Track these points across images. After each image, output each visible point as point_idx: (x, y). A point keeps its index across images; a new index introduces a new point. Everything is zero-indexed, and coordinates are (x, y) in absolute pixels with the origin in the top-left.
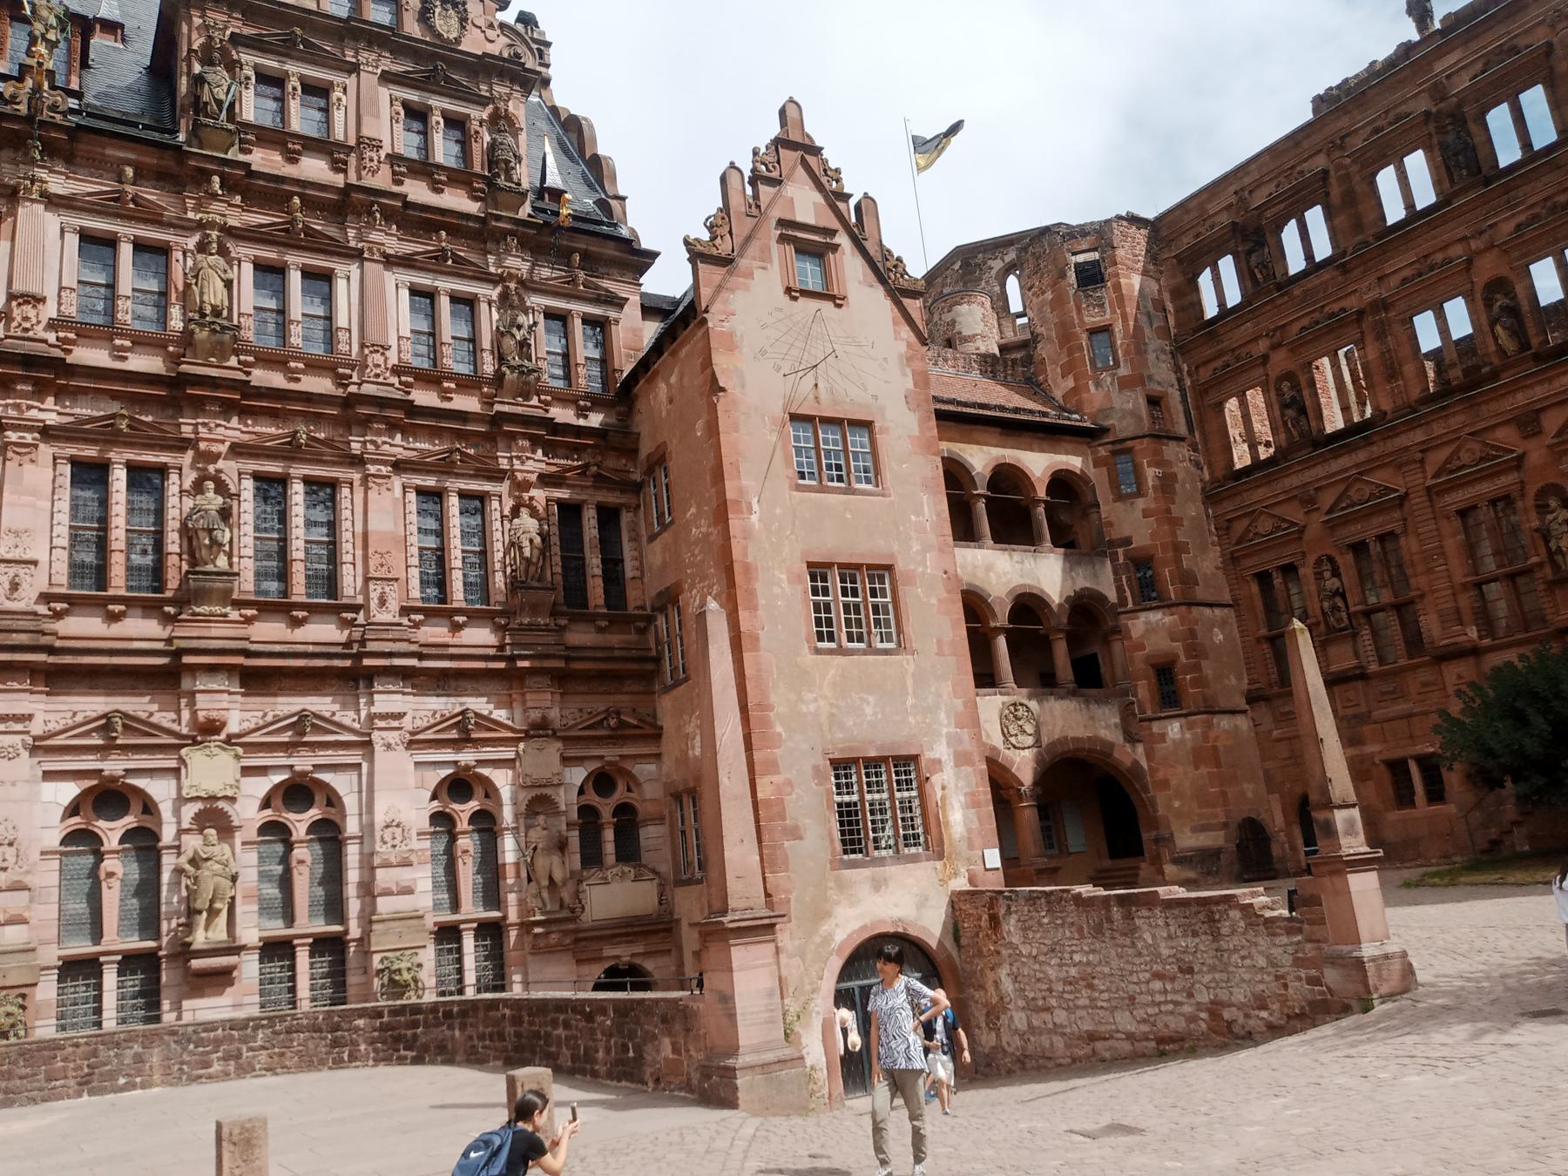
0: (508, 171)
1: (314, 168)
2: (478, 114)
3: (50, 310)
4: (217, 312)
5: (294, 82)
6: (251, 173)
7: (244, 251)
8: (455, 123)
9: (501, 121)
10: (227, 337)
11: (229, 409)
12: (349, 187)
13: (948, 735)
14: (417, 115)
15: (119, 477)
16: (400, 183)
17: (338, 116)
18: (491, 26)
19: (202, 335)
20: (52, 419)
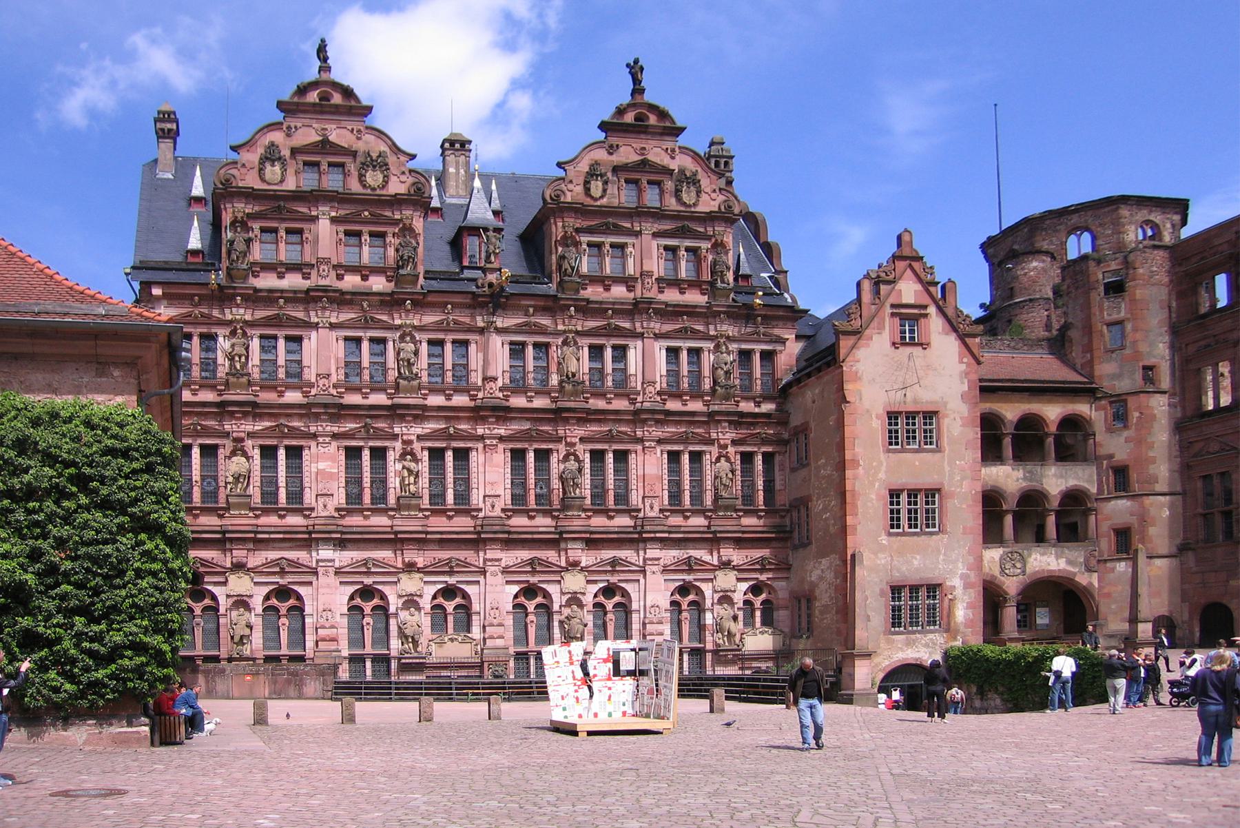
0: (722, 276)
1: (619, 291)
2: (705, 245)
3: (500, 383)
4: (574, 375)
5: (607, 246)
6: (588, 301)
7: (585, 342)
8: (693, 251)
9: (719, 246)
10: (580, 387)
11: (582, 421)
12: (636, 303)
13: (962, 575)
14: (672, 250)
15: (531, 457)
16: (662, 292)
17: (630, 261)
18: (714, 191)
19: (568, 387)
20: (502, 432)
